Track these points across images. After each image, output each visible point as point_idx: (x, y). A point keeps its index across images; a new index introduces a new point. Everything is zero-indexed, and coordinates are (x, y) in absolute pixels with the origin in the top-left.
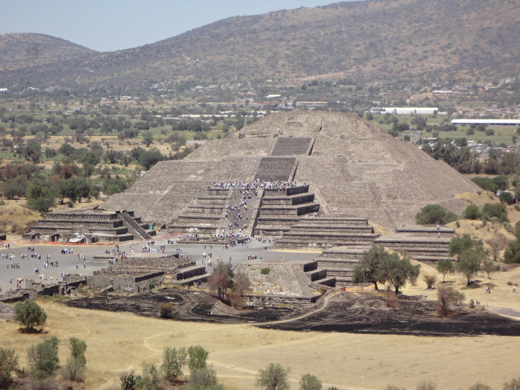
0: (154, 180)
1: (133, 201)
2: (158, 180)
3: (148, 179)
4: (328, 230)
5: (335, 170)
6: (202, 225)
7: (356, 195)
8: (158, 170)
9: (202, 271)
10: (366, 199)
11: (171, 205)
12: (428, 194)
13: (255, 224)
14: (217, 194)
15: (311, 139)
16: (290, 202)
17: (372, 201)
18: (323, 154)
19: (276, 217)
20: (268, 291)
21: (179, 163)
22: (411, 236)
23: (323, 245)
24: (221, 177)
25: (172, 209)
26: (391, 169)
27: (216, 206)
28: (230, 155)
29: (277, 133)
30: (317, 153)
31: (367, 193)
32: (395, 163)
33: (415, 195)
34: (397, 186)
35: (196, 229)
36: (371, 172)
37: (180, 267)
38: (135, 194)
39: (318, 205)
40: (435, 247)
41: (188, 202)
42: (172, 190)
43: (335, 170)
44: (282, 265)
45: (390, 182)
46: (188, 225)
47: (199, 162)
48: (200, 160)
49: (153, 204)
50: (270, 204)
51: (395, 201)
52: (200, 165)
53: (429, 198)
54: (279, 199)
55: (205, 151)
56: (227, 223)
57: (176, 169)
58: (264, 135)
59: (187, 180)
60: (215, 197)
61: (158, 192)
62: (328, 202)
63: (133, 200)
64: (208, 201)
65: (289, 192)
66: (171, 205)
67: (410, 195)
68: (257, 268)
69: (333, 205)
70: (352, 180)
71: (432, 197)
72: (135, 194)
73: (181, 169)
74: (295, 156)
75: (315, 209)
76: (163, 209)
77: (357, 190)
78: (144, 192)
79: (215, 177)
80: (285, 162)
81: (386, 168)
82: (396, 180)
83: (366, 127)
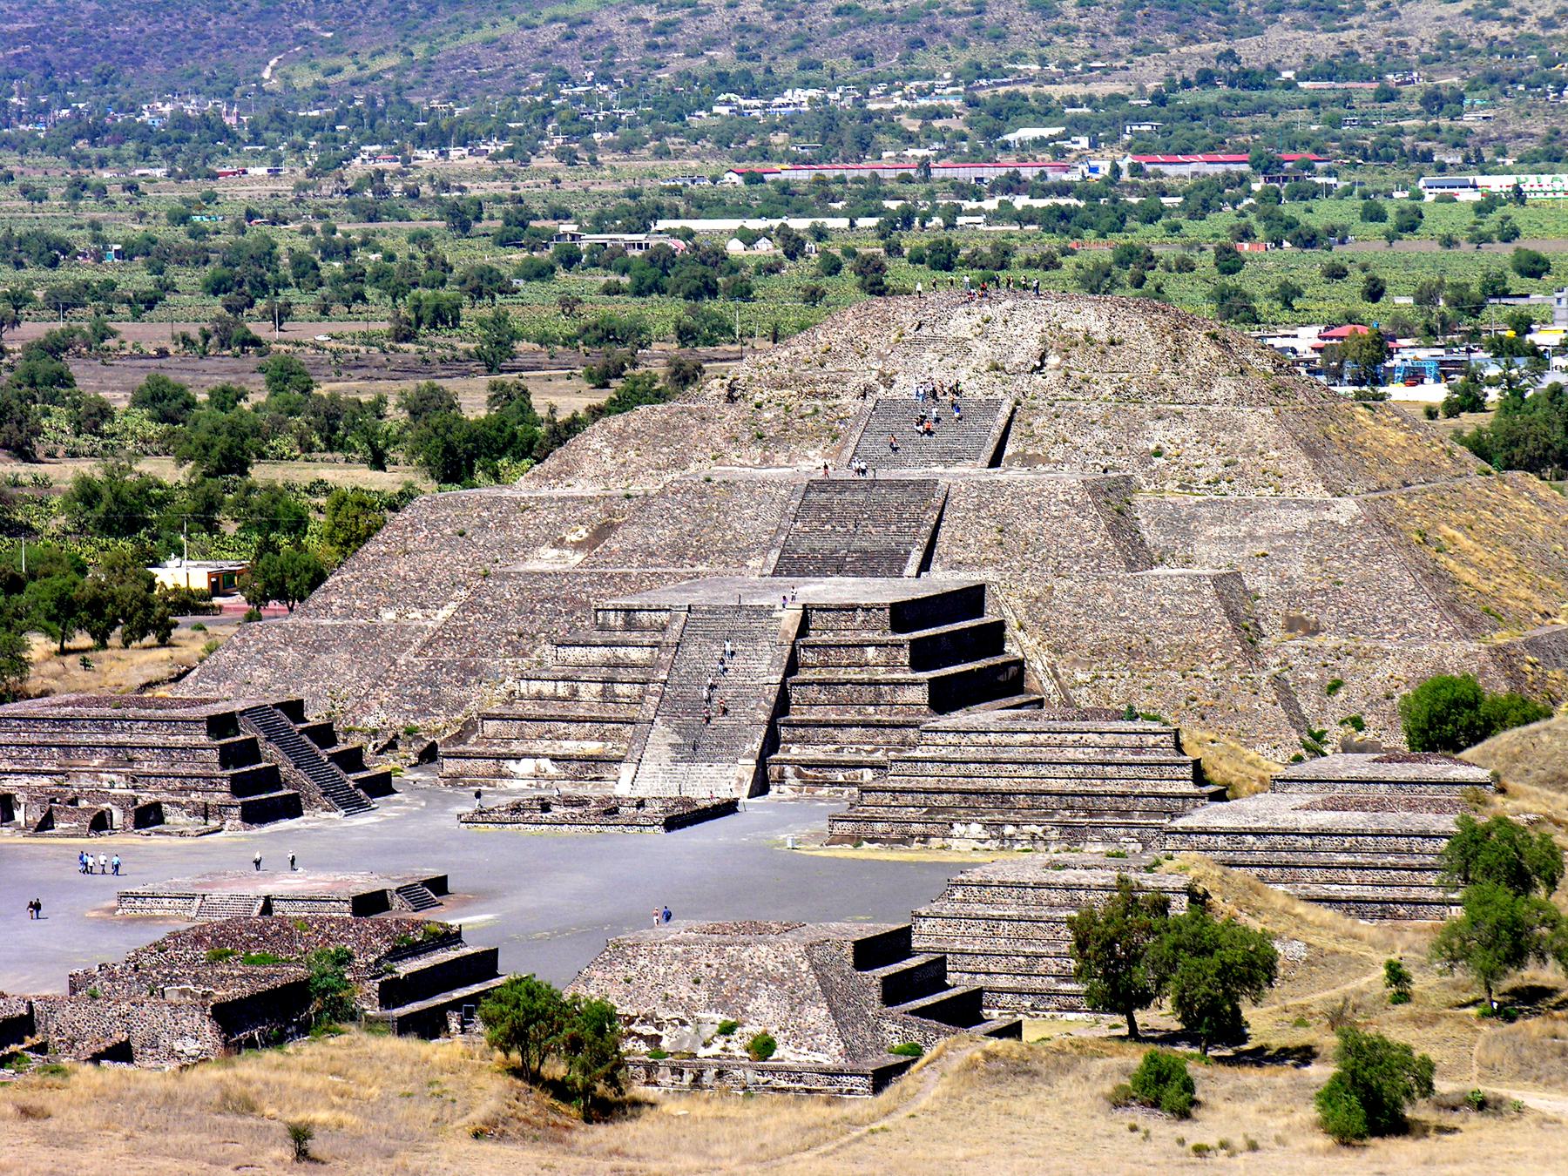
0: (401, 567)
1: (317, 651)
2: (415, 570)
3: (376, 563)
4: (1029, 771)
5: (1087, 524)
6: (569, 747)
7: (1165, 623)
8: (416, 530)
9: (484, 965)
10: (1198, 638)
11: (463, 668)
12: (1442, 616)
13: (772, 743)
14: (629, 626)
15: (999, 403)
16: (904, 656)
17: (1225, 645)
18: (1046, 461)
19: (851, 715)
20: (715, 1049)
21: (497, 500)
22: (1309, 808)
23: (1009, 830)
24: (652, 554)
25: (464, 683)
26: (1303, 519)
27: (623, 674)
28: (693, 467)
29: (871, 379)
30: (1028, 461)
31: (1205, 615)
32: (1318, 493)
33: (1394, 620)
34: (1324, 585)
35: (545, 763)
36: (1227, 530)
37: (397, 954)
38: (327, 622)
39: (1020, 664)
40: (1398, 852)
41: (525, 655)
42: (465, 607)
43: (1087, 524)
44: (769, 944)
45: (1297, 569)
46: (516, 747)
47: (573, 499)
48: (577, 491)
49: (394, 663)
50: (825, 665)
51: (1314, 642)
52: (576, 509)
53: (1446, 629)
54: (861, 646)
55: (598, 453)
56: (662, 737)
57: (484, 526)
58: (820, 389)
59: (522, 568)
60: (618, 636)
61: (417, 614)
62: (1058, 650)
63: (321, 647)
64: (596, 654)
65: (904, 615)
66: (463, 668)
67: (1375, 618)
68: (675, 956)
69: (1075, 661)
70: (1152, 564)
71: (1459, 625)
72: (327, 622)
73: (504, 525)
74: (940, 469)
75: (1006, 683)
76: (432, 684)
77: (1167, 604)
78: (363, 614)
79: (628, 554)
80: (894, 497)
81: (1282, 513)
82: (1320, 562)
83: (1214, 352)
